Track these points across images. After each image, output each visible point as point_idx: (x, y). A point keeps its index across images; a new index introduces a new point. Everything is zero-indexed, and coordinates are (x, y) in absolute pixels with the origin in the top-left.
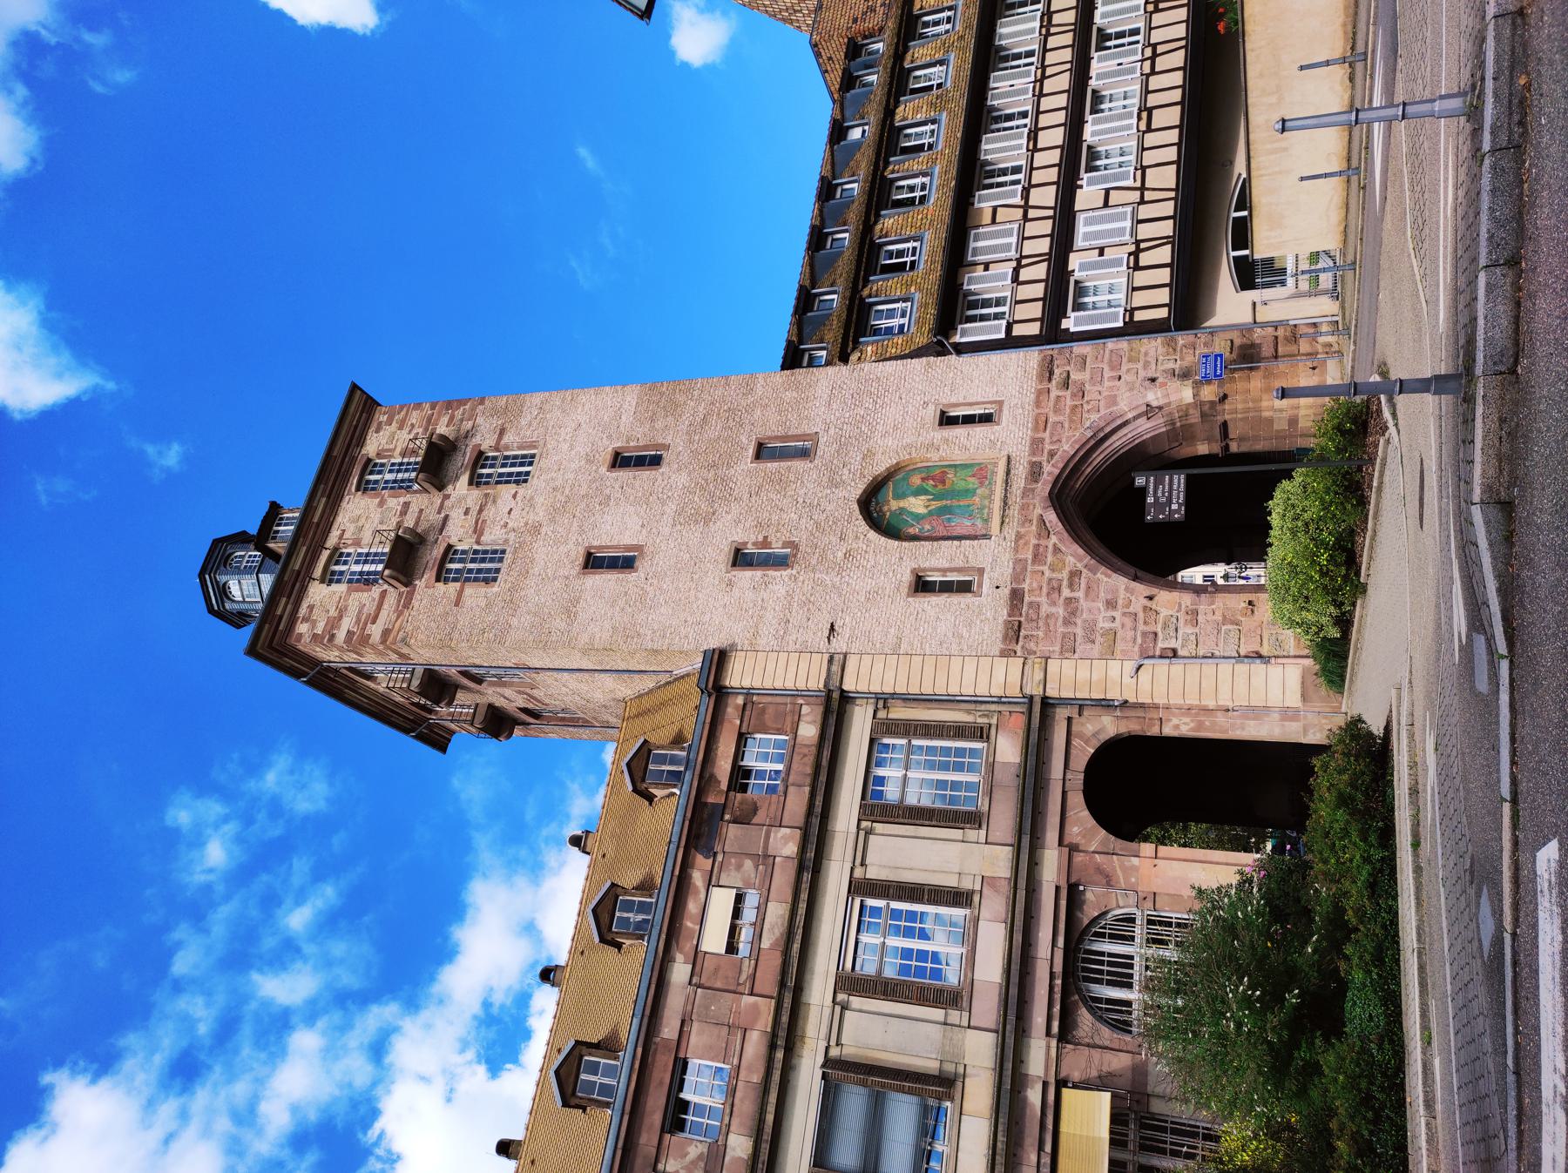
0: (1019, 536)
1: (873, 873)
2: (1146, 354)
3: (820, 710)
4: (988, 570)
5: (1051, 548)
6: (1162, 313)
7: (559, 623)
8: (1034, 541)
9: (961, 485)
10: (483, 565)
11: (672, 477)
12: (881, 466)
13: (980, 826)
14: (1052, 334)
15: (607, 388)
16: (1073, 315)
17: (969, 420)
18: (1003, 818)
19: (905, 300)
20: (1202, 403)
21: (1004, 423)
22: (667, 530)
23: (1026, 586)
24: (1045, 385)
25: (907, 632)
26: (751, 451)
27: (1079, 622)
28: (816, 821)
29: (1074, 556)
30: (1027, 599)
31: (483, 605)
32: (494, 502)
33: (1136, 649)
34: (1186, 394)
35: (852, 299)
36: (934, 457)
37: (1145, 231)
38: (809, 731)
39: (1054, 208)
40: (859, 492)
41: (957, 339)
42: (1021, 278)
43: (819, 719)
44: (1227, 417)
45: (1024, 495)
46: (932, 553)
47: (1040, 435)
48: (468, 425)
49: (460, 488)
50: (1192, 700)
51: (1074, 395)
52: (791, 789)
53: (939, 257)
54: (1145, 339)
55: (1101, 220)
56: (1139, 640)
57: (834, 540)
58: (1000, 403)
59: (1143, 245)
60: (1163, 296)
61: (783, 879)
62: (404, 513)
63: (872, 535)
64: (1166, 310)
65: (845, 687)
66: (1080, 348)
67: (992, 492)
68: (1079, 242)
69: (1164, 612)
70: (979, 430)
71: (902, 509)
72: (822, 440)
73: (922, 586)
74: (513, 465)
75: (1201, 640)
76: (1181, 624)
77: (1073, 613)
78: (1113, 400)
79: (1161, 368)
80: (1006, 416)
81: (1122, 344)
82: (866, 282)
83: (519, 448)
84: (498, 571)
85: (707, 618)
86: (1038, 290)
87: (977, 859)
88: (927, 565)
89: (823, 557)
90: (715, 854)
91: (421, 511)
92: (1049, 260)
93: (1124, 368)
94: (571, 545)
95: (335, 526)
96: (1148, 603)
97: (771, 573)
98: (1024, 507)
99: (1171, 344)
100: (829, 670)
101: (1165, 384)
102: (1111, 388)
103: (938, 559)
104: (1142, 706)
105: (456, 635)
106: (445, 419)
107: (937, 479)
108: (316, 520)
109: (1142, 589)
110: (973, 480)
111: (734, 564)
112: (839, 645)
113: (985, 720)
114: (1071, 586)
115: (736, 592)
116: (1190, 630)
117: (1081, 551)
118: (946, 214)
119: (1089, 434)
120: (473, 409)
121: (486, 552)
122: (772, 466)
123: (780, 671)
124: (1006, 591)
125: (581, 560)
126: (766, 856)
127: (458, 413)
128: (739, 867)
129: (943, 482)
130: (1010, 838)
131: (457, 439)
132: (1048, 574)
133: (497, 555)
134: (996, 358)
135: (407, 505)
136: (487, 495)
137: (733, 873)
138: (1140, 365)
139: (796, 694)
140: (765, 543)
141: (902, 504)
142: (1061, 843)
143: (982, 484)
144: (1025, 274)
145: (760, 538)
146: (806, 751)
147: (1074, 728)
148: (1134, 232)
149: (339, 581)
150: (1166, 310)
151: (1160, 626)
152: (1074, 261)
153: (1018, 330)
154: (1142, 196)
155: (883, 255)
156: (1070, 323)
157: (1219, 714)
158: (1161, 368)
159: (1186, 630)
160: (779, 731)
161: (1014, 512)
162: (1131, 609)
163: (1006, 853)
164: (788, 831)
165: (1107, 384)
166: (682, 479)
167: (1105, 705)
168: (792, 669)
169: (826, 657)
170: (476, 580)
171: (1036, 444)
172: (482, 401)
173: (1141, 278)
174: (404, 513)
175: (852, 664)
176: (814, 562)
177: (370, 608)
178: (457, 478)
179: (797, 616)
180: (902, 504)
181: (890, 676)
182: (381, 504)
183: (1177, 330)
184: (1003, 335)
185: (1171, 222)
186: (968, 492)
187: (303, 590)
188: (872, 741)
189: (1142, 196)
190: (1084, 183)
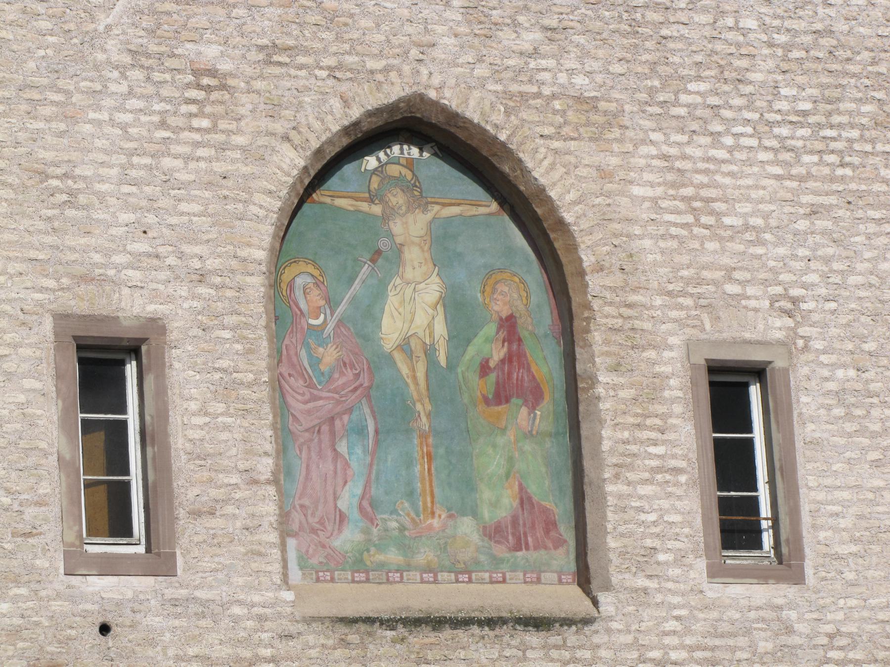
9: (491, 461)
21: (714, 591)
40: (451, 100)
46: (227, 390)
67: (464, 571)
73: (102, 365)
110: (508, 502)
141: (415, 258)
143: (494, 533)
180: (415, 258)
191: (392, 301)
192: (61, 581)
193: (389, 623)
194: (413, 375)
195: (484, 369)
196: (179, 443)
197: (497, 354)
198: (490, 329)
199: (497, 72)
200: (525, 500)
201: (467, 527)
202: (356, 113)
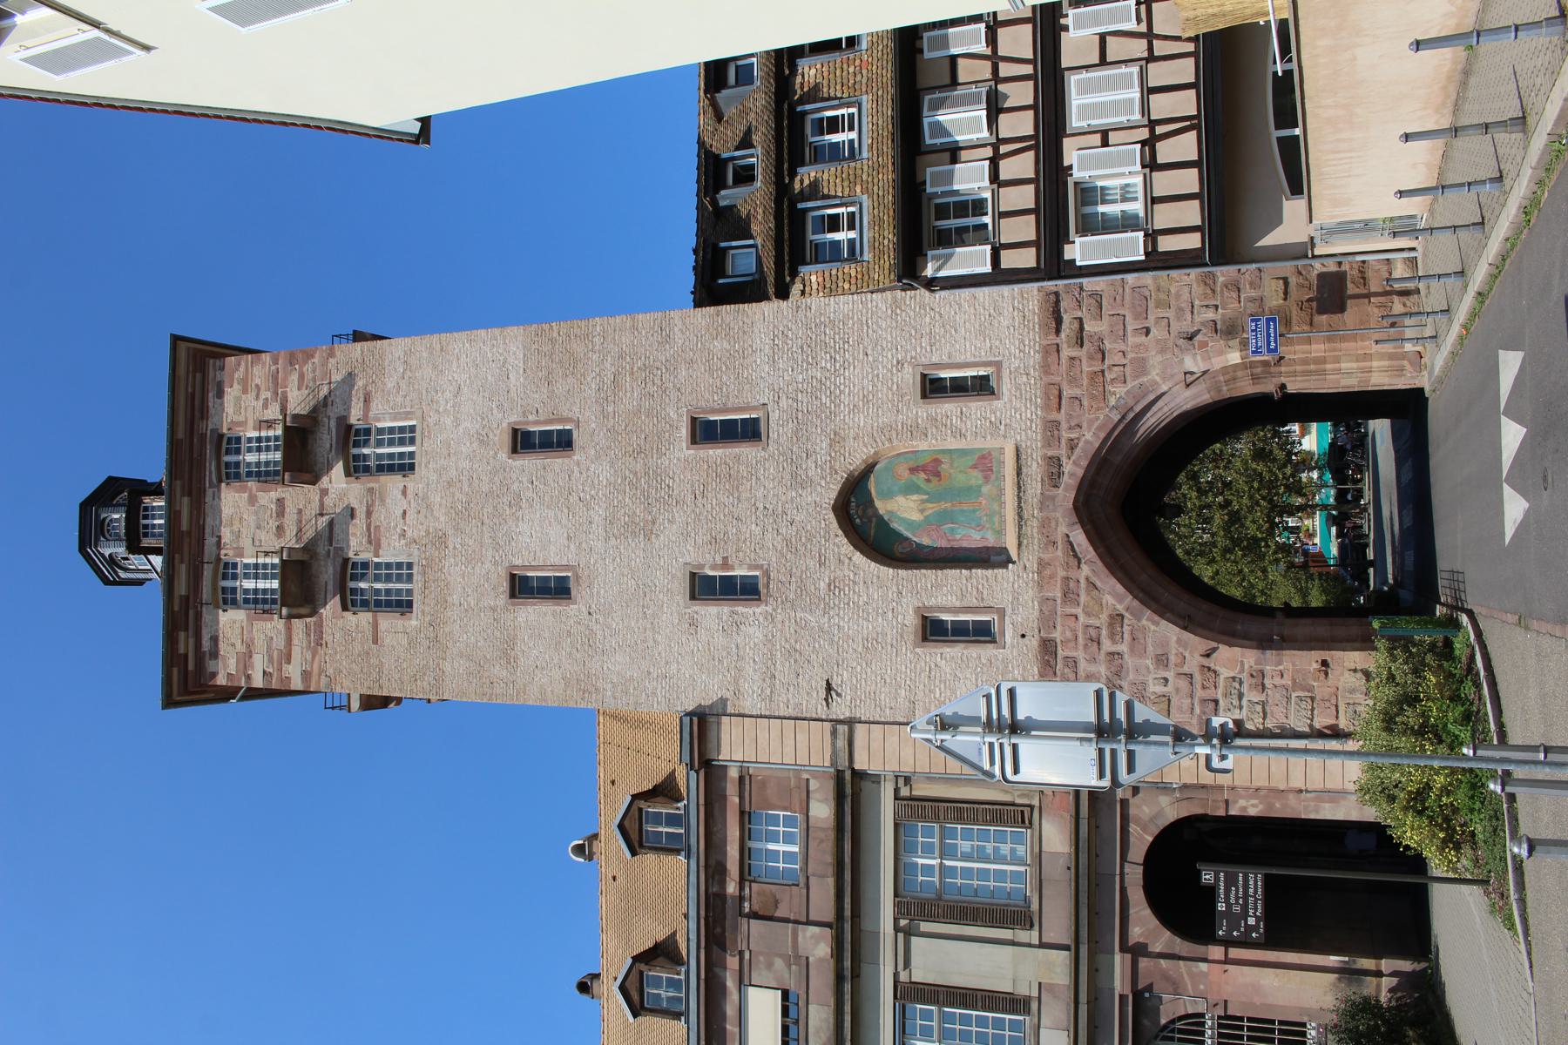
0: (1042, 565)
1: (919, 975)
2: (1178, 296)
3: (830, 785)
4: (1009, 611)
5: (1083, 581)
6: (1193, 241)
7: (498, 671)
8: (1061, 573)
9: (960, 479)
10: (391, 586)
11: (588, 466)
12: (855, 460)
13: (1032, 926)
14: (1053, 265)
15: (482, 333)
16: (1078, 240)
17: (959, 388)
18: (1058, 919)
19: (852, 204)
20: (1252, 365)
21: (1006, 399)
22: (599, 545)
23: (1057, 635)
24: (1052, 339)
25: (920, 695)
26: (684, 431)
27: (1124, 684)
28: (848, 927)
29: (1114, 595)
30: (1060, 652)
31: (405, 642)
32: (382, 500)
33: (1195, 721)
34: (1234, 357)
35: (778, 201)
36: (923, 446)
37: (1162, 106)
38: (822, 811)
39: (1033, 62)
40: (834, 495)
41: (929, 272)
42: (1003, 176)
43: (831, 795)
44: (1283, 380)
45: (1042, 506)
46: (937, 586)
47: (1054, 416)
48: (325, 391)
49: (336, 478)
50: (1263, 783)
51: (1091, 358)
52: (812, 880)
53: (888, 148)
54: (1174, 273)
55: (1101, 86)
56: (1197, 711)
57: (812, 563)
58: (998, 365)
59: (1159, 130)
60: (1191, 213)
61: (822, 982)
62: (281, 512)
63: (858, 558)
64: (1198, 235)
65: (857, 767)
66: (1088, 283)
67: (1001, 492)
68: (1075, 121)
69: (1225, 673)
70: (975, 408)
71: (890, 512)
72: (774, 416)
73: (933, 630)
74: (391, 443)
75: (1268, 709)
76: (1245, 689)
77: (1118, 674)
78: (1141, 367)
79: (1198, 319)
80: (1006, 387)
81: (1147, 278)
82: (793, 174)
83: (395, 419)
84: (410, 592)
85: (674, 667)
86: (1024, 197)
87: (1028, 965)
88: (932, 602)
89: (802, 588)
90: (741, 953)
91: (300, 511)
92: (1035, 147)
93: (1152, 318)
94: (488, 565)
95: (208, 530)
96: (1205, 662)
97: (740, 609)
98: (1044, 524)
99: (1208, 282)
100: (834, 745)
101: (1204, 345)
102: (1138, 346)
103: (949, 592)
104: (1204, 787)
105: (384, 681)
106: (295, 377)
107: (931, 468)
108: (184, 527)
109: (1197, 643)
110: (975, 473)
111: (693, 597)
112: (841, 710)
113: (1026, 801)
114: (1112, 636)
115: (702, 633)
116: (1256, 697)
117: (1120, 588)
118: (888, 75)
119: (1116, 418)
120: (324, 364)
121: (388, 566)
122: (716, 453)
123: (775, 744)
124: (1033, 642)
125: (505, 585)
126: (797, 957)
127: (308, 368)
128: (770, 966)
129: (938, 474)
130: (1066, 939)
131: (315, 410)
132: (1082, 618)
133: (403, 570)
134: (983, 293)
135: (280, 502)
136: (371, 490)
137: (764, 972)
138: (1171, 314)
139: (798, 770)
140: (725, 564)
142: (1122, 950)
144: (1008, 169)
145: (719, 561)
146: (822, 835)
147: (1132, 811)
148: (1145, 108)
149: (234, 603)
150: (1198, 235)
151: (1220, 691)
152: (1072, 153)
153: (1010, 260)
154: (1150, 48)
155: (808, 130)
156: (1079, 250)
157: (1291, 796)
158: (1198, 319)
159: (1251, 696)
160: (785, 809)
161: (1032, 528)
162: (1186, 669)
163: (1062, 958)
164: (816, 929)
165: (1131, 340)
166: (603, 472)
167: (1163, 788)
168: (789, 742)
169: (828, 725)
170: (389, 604)
171: (1051, 428)
172: (331, 354)
173: (1165, 183)
174: (281, 512)
175: (860, 730)
176: (792, 596)
177: (279, 642)
178: (330, 467)
179: (783, 669)
181: (907, 753)
182: (252, 500)
183: (1214, 265)
184: (988, 269)
185: (1193, 92)
186: (971, 491)
187: (198, 616)
188: (896, 825)
189: (1150, 48)
190: (1069, 21)
191: (905, 515)
192: (1007, 651)
193: (1020, 527)
194: (932, 508)
195: (928, 481)
196: (958, 604)
197: (923, 475)
198: (914, 478)
199: (823, 478)
200: (974, 467)
201: (985, 490)
202: (840, 532)
